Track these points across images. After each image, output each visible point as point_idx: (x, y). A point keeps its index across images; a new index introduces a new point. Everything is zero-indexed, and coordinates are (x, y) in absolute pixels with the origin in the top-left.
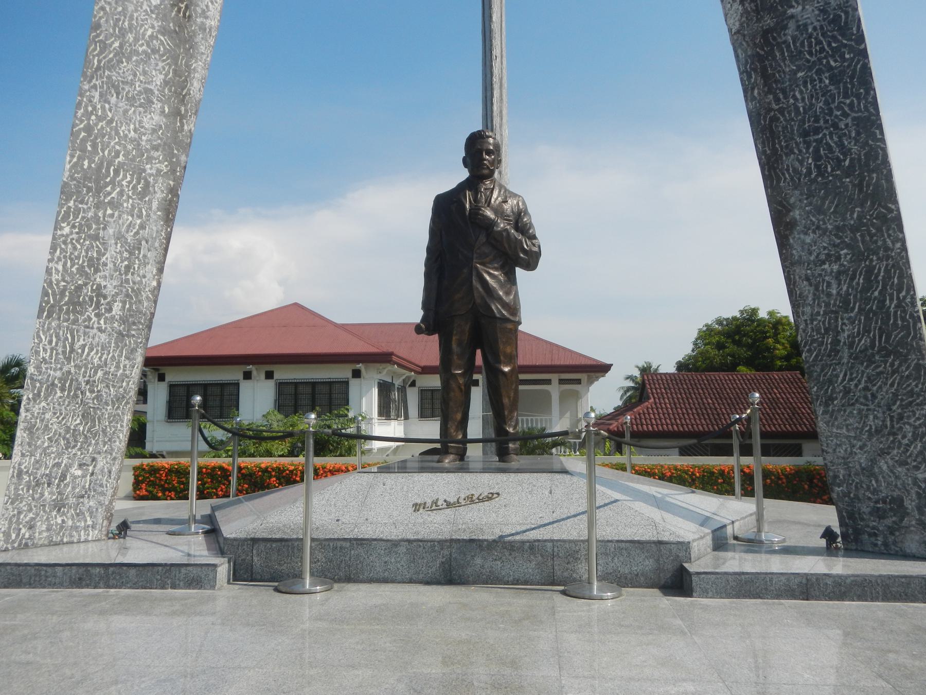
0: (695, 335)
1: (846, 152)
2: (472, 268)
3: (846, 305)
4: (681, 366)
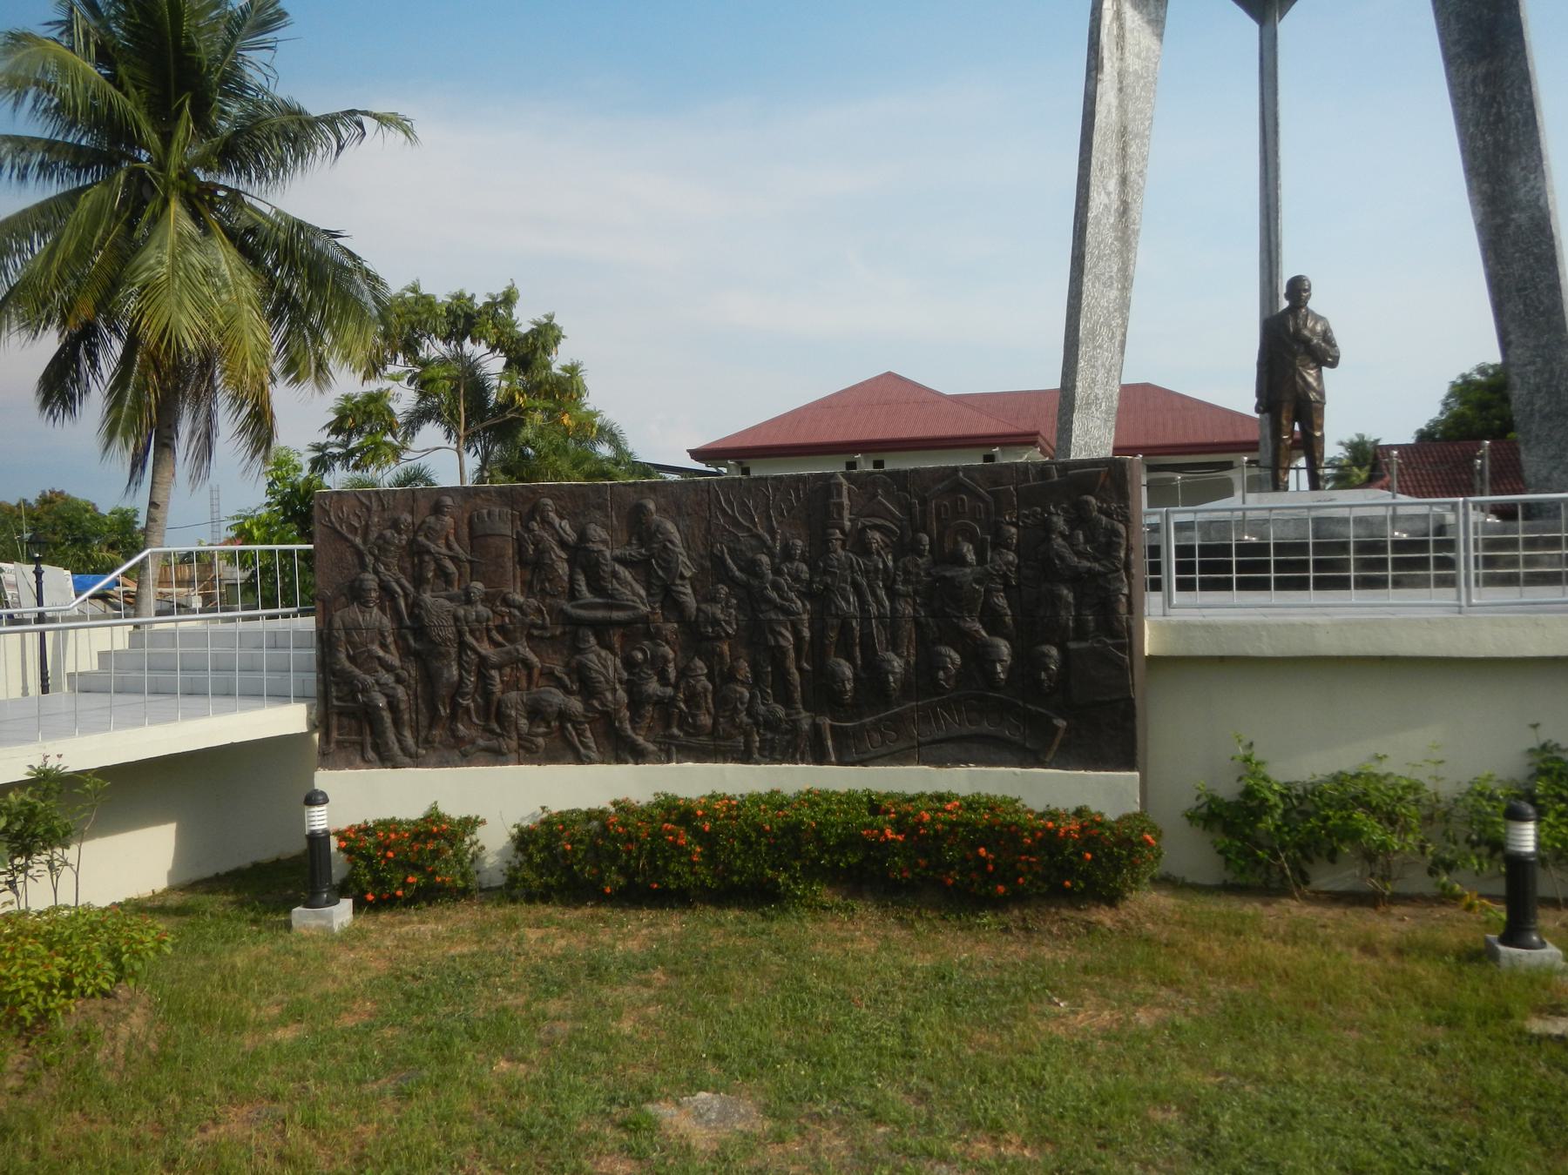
0: (1444, 390)
1: (1541, 303)
2: (1295, 370)
3: (1538, 390)
4: (1423, 436)
